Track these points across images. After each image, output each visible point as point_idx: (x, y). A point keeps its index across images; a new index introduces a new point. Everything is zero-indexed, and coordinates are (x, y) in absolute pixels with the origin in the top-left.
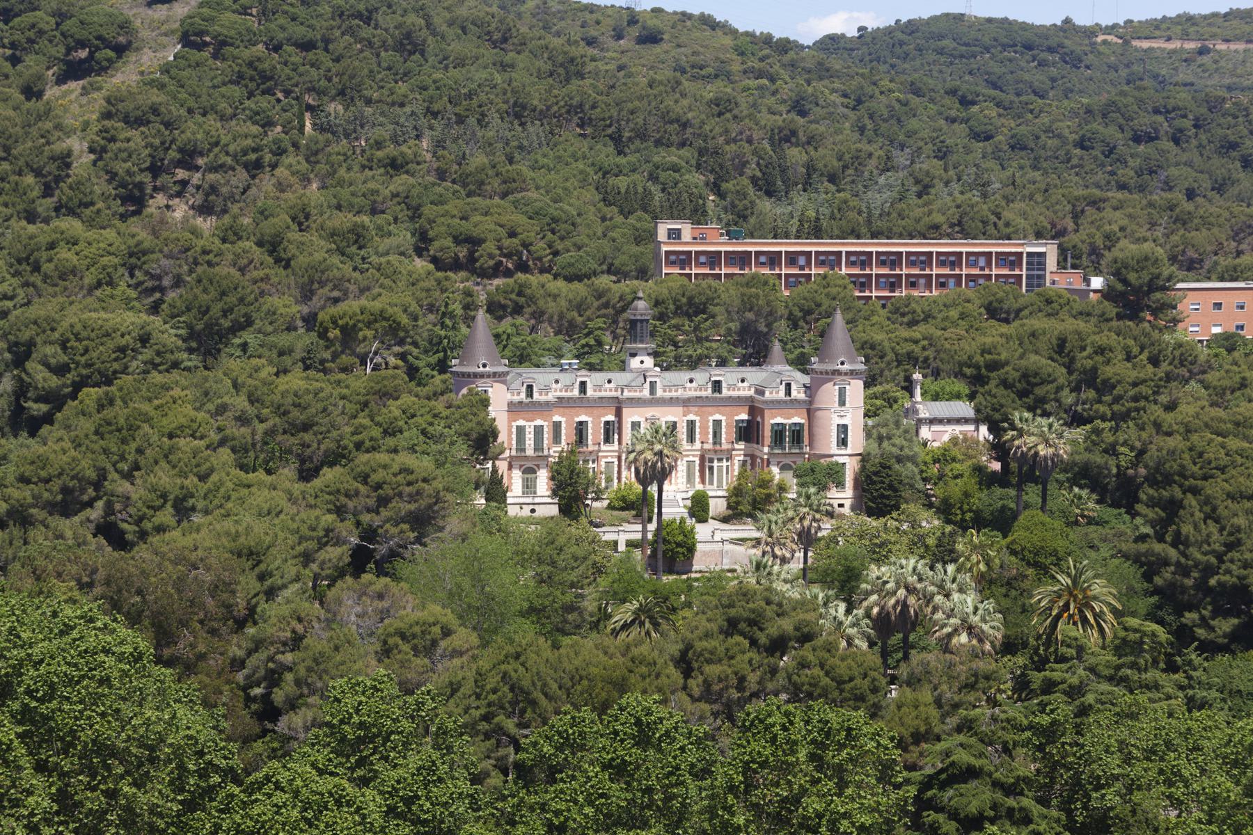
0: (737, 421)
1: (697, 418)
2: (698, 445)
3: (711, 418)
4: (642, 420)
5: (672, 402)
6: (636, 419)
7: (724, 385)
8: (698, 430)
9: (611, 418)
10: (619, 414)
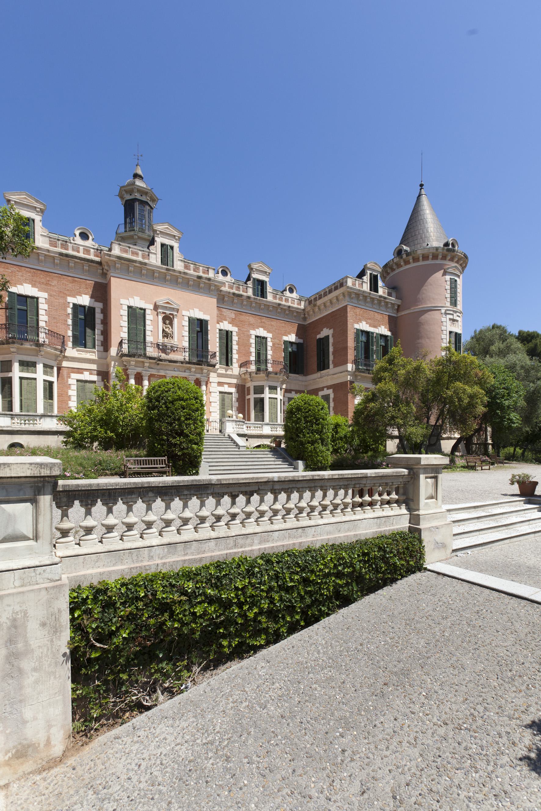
0: (285, 342)
1: (234, 329)
3: (253, 333)
4: (149, 307)
6: (137, 302)
7: (269, 289)
8: (235, 347)
9: (85, 300)
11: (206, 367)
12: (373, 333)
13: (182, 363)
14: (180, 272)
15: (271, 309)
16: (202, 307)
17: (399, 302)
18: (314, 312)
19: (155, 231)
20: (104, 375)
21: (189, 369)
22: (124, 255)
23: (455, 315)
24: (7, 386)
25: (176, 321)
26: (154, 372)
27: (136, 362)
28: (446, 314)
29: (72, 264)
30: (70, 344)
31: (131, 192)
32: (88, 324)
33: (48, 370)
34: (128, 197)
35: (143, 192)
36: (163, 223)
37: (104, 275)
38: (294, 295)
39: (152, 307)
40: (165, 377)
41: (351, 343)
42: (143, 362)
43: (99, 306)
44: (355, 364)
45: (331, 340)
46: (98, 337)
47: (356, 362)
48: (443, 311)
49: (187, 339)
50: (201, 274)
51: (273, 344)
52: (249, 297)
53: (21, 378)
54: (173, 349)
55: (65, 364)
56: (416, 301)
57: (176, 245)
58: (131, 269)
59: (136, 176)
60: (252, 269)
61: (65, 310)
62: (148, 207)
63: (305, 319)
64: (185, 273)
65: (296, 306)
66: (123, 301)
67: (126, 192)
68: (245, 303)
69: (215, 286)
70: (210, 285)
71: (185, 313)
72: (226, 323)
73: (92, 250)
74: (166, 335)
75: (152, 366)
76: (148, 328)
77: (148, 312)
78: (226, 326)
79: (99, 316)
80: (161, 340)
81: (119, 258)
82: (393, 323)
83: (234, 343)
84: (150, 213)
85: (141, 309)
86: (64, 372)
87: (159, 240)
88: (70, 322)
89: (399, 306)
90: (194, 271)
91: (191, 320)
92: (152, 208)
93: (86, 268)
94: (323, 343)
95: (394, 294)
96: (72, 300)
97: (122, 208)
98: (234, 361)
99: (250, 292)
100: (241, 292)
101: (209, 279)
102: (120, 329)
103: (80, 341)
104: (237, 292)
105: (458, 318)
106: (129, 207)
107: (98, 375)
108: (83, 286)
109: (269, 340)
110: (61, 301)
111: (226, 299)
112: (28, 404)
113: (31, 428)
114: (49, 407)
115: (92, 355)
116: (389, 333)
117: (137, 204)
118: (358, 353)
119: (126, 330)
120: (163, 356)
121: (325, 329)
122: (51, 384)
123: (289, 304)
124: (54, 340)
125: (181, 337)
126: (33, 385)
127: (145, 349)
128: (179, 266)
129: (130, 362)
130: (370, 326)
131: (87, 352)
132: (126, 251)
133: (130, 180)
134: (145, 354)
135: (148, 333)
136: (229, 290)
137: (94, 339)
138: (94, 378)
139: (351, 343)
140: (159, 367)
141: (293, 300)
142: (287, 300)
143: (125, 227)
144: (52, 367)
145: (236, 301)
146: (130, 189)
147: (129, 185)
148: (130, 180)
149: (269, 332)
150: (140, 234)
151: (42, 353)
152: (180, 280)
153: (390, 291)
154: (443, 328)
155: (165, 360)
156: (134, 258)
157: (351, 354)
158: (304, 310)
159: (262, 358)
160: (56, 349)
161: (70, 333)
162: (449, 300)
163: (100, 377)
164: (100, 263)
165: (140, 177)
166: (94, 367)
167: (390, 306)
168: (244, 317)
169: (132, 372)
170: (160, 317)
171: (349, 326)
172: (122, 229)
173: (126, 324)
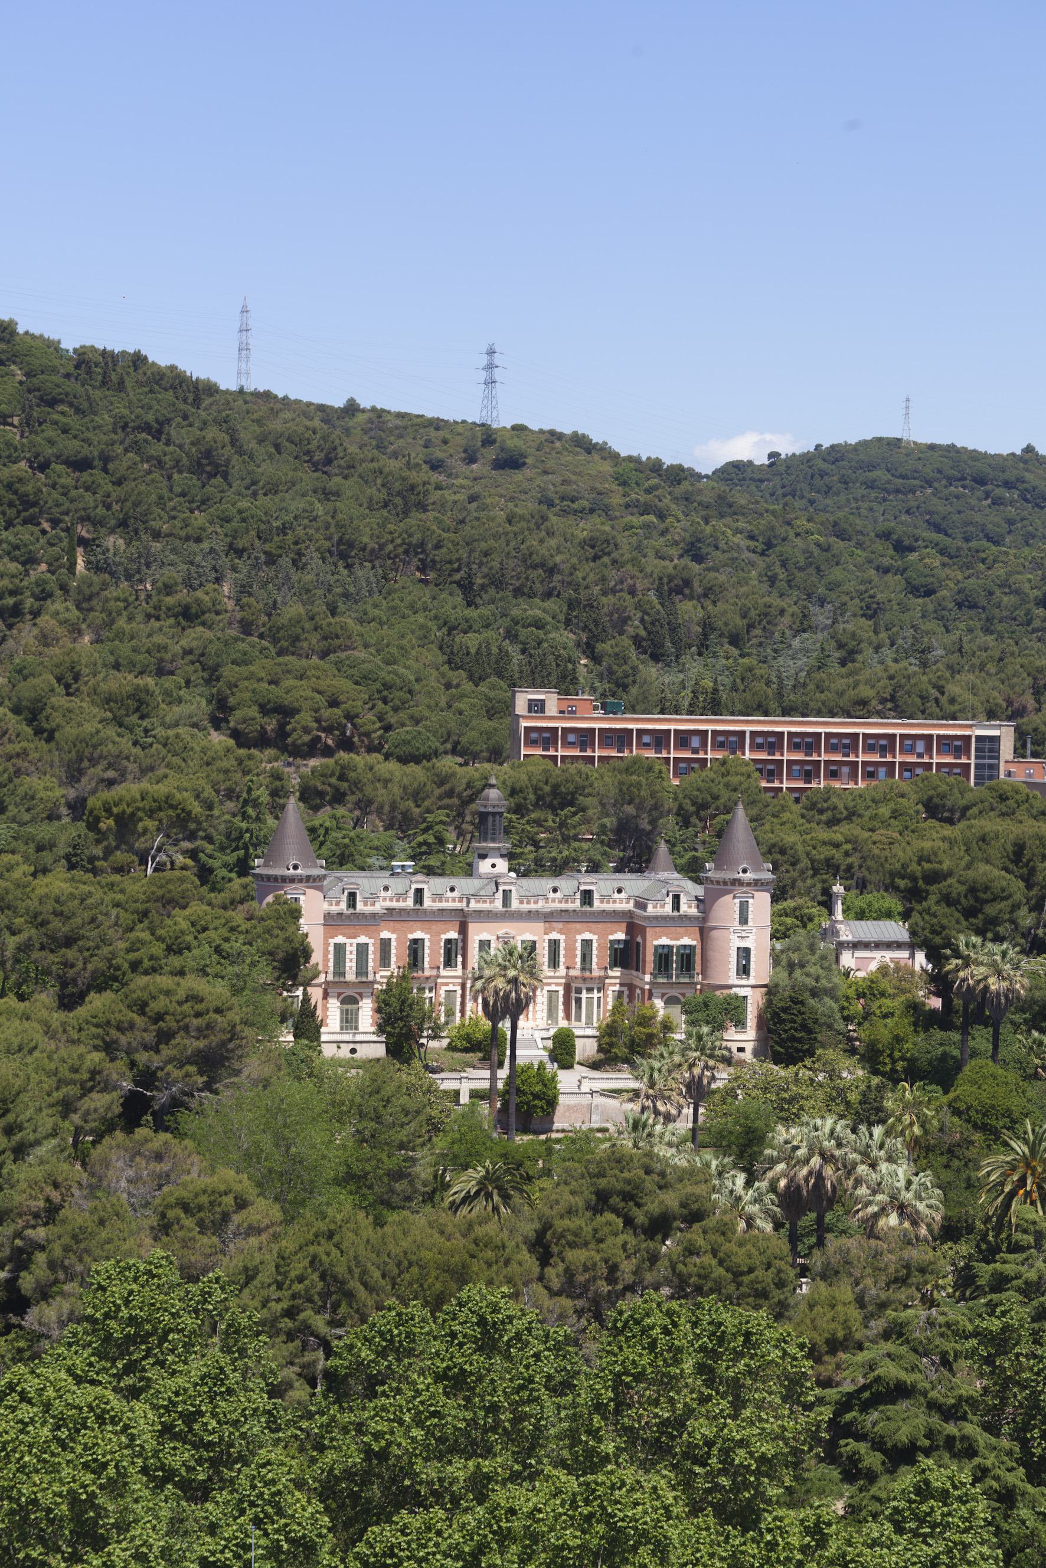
0: (612, 942)
1: (562, 938)
2: (562, 971)
3: (579, 938)
4: (493, 938)
6: (485, 936)
7: (596, 896)
8: (562, 952)
9: (453, 935)
10: (463, 930)
38: (623, 895)
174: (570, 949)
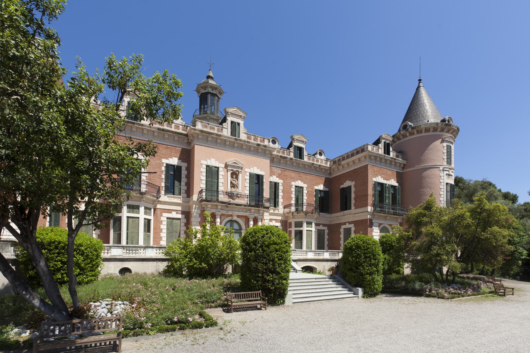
1: (280, 181)
2: (281, 209)
3: (294, 184)
4: (221, 166)
5: (259, 151)
6: (213, 163)
7: (305, 153)
8: (281, 194)
10: (187, 156)
11: (262, 209)
12: (386, 184)
13: (245, 206)
14: (245, 141)
15: (307, 167)
16: (258, 166)
17: (404, 162)
18: (338, 169)
19: (227, 113)
20: (187, 214)
21: (250, 210)
22: (205, 129)
23: (450, 171)
24: (117, 223)
25: (240, 176)
26: (224, 212)
27: (212, 205)
28: (443, 170)
29: (166, 136)
30: (163, 192)
31: (205, 88)
32: (177, 178)
33: (148, 211)
34: (203, 91)
35: (213, 87)
36: (233, 107)
37: (189, 143)
38: (323, 157)
39: (223, 166)
40: (231, 216)
41: (370, 192)
42: (217, 205)
43: (184, 165)
44: (373, 206)
45: (353, 189)
46: (184, 187)
47: (374, 205)
48: (441, 168)
49: (248, 188)
50: (259, 142)
51: (308, 192)
52: (291, 159)
53: (128, 217)
54: (238, 196)
55: (159, 206)
56: (420, 162)
57: (242, 122)
58: (210, 139)
59: (209, 77)
60: (294, 139)
61: (161, 168)
62: (216, 98)
63: (330, 174)
64: (248, 142)
65: (324, 165)
66: (203, 162)
67: (202, 88)
68: (288, 163)
69: (269, 151)
70: (265, 151)
71: (247, 170)
72: (274, 177)
73: (181, 126)
74: (233, 186)
75: (223, 208)
76: (220, 181)
77: (220, 169)
78: (275, 179)
79: (184, 172)
80: (229, 189)
81: (202, 131)
82: (400, 177)
83: (280, 191)
84: (218, 101)
85: (216, 167)
86: (158, 212)
87: (230, 119)
88: (163, 176)
89: (404, 165)
90: (254, 140)
91: (251, 175)
92: (219, 98)
93: (176, 138)
94: (346, 193)
95: (400, 156)
96: (165, 161)
97: (198, 99)
98: (280, 203)
99: (292, 155)
100: (285, 155)
101: (265, 146)
102: (200, 182)
103: (170, 190)
104: (283, 155)
105: (452, 174)
106: (203, 99)
107: (182, 214)
108: (174, 151)
109: (305, 189)
110: (158, 162)
111: (275, 160)
112: (132, 238)
113: (137, 256)
114: (147, 238)
115: (178, 200)
116: (397, 184)
117: (209, 96)
118: (375, 198)
119: (204, 182)
120: (232, 201)
121: (347, 182)
122: (149, 221)
123: (319, 163)
124: (152, 190)
125: (244, 187)
126: (137, 222)
127: (218, 196)
128: (243, 136)
129: (207, 205)
130: (384, 179)
131: (175, 198)
132: (206, 127)
133: (205, 80)
134: (218, 200)
135: (220, 184)
136: (277, 154)
137: (180, 188)
138: (179, 216)
139: (370, 192)
140: (228, 209)
141: (321, 160)
142: (317, 161)
143: (200, 112)
144: (150, 209)
145: (282, 161)
146: (205, 86)
147: (203, 83)
148: (205, 80)
149: (304, 183)
150: (211, 116)
151: (144, 199)
152: (244, 147)
153: (398, 154)
154: (441, 181)
155: (233, 204)
156: (212, 131)
157: (370, 200)
158: (330, 168)
159: (300, 202)
160: (154, 196)
161: (163, 184)
162: (446, 160)
163: (184, 216)
164: (187, 135)
165: (212, 78)
166: (179, 208)
167: (398, 165)
168: (288, 173)
169: (208, 213)
170: (229, 173)
171: (369, 180)
172: (198, 113)
173: (204, 178)
174: (287, 192)
